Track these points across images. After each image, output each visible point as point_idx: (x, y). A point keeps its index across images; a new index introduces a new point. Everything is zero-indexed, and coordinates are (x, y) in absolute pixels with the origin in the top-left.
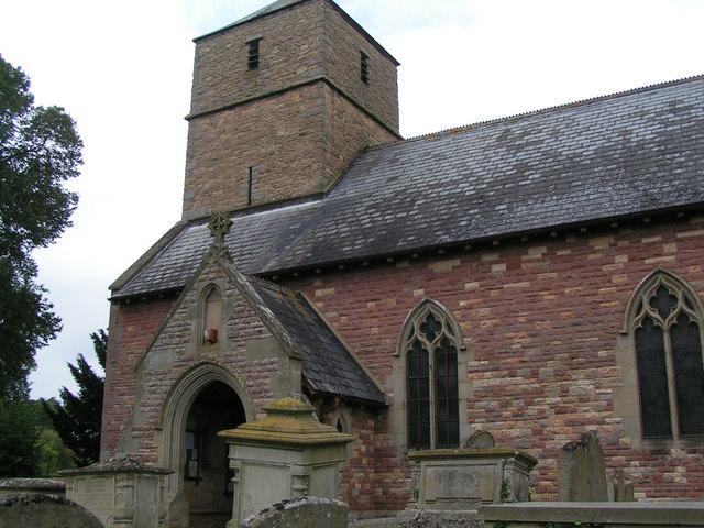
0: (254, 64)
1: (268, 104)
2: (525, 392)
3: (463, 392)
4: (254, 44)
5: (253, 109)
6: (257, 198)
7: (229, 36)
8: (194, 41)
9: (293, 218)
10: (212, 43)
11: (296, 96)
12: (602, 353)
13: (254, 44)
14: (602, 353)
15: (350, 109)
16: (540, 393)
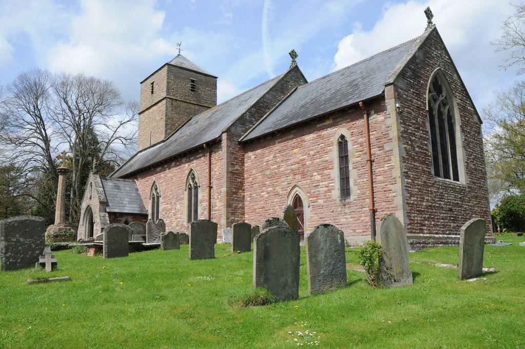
0: (152, 92)
1: (155, 108)
2: (169, 209)
3: (160, 210)
4: (152, 84)
5: (151, 110)
6: (153, 143)
7: (148, 81)
8: (141, 83)
9: (153, 152)
10: (144, 84)
11: (160, 104)
12: (182, 196)
13: (152, 84)
14: (182, 196)
15: (183, 105)
16: (171, 209)
